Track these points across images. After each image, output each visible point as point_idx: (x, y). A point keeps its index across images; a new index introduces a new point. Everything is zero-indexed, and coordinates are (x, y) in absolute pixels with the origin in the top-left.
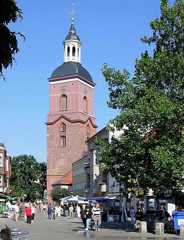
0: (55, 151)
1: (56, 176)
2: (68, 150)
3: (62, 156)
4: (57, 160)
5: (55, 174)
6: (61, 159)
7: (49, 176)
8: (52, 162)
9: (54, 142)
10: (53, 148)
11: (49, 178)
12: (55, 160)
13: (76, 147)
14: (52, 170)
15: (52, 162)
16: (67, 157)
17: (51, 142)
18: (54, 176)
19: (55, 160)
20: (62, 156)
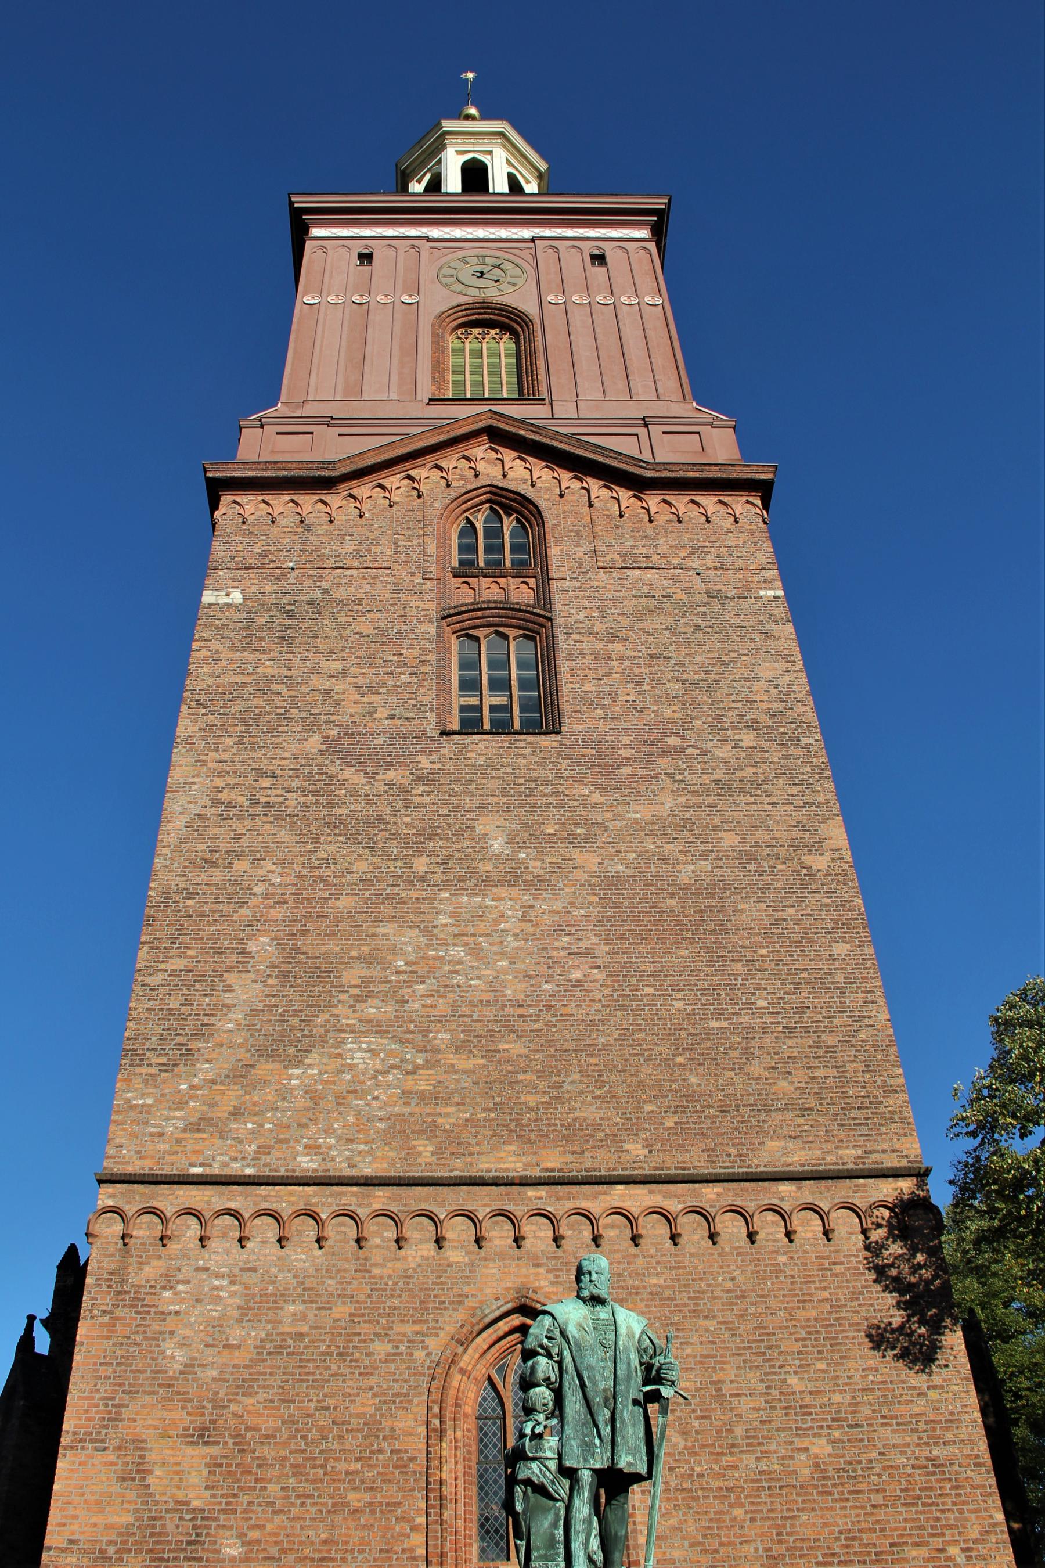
0: (352, 776)
1: (349, 1197)
2: (610, 773)
3: (497, 845)
4: (386, 911)
5: (307, 1164)
6: (485, 885)
7: (169, 1199)
8: (262, 945)
9: (338, 666)
10: (314, 743)
11: (145, 1230)
12: (345, 902)
13: (748, 739)
14: (240, 1075)
15: (262, 945)
16: (590, 861)
17: (269, 669)
18: (286, 1200)
19: (345, 902)
20: (497, 845)
